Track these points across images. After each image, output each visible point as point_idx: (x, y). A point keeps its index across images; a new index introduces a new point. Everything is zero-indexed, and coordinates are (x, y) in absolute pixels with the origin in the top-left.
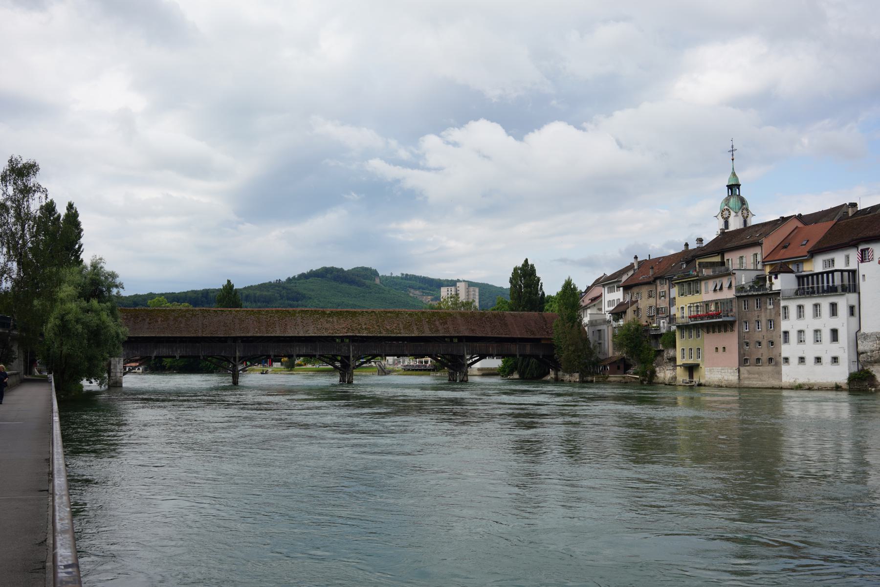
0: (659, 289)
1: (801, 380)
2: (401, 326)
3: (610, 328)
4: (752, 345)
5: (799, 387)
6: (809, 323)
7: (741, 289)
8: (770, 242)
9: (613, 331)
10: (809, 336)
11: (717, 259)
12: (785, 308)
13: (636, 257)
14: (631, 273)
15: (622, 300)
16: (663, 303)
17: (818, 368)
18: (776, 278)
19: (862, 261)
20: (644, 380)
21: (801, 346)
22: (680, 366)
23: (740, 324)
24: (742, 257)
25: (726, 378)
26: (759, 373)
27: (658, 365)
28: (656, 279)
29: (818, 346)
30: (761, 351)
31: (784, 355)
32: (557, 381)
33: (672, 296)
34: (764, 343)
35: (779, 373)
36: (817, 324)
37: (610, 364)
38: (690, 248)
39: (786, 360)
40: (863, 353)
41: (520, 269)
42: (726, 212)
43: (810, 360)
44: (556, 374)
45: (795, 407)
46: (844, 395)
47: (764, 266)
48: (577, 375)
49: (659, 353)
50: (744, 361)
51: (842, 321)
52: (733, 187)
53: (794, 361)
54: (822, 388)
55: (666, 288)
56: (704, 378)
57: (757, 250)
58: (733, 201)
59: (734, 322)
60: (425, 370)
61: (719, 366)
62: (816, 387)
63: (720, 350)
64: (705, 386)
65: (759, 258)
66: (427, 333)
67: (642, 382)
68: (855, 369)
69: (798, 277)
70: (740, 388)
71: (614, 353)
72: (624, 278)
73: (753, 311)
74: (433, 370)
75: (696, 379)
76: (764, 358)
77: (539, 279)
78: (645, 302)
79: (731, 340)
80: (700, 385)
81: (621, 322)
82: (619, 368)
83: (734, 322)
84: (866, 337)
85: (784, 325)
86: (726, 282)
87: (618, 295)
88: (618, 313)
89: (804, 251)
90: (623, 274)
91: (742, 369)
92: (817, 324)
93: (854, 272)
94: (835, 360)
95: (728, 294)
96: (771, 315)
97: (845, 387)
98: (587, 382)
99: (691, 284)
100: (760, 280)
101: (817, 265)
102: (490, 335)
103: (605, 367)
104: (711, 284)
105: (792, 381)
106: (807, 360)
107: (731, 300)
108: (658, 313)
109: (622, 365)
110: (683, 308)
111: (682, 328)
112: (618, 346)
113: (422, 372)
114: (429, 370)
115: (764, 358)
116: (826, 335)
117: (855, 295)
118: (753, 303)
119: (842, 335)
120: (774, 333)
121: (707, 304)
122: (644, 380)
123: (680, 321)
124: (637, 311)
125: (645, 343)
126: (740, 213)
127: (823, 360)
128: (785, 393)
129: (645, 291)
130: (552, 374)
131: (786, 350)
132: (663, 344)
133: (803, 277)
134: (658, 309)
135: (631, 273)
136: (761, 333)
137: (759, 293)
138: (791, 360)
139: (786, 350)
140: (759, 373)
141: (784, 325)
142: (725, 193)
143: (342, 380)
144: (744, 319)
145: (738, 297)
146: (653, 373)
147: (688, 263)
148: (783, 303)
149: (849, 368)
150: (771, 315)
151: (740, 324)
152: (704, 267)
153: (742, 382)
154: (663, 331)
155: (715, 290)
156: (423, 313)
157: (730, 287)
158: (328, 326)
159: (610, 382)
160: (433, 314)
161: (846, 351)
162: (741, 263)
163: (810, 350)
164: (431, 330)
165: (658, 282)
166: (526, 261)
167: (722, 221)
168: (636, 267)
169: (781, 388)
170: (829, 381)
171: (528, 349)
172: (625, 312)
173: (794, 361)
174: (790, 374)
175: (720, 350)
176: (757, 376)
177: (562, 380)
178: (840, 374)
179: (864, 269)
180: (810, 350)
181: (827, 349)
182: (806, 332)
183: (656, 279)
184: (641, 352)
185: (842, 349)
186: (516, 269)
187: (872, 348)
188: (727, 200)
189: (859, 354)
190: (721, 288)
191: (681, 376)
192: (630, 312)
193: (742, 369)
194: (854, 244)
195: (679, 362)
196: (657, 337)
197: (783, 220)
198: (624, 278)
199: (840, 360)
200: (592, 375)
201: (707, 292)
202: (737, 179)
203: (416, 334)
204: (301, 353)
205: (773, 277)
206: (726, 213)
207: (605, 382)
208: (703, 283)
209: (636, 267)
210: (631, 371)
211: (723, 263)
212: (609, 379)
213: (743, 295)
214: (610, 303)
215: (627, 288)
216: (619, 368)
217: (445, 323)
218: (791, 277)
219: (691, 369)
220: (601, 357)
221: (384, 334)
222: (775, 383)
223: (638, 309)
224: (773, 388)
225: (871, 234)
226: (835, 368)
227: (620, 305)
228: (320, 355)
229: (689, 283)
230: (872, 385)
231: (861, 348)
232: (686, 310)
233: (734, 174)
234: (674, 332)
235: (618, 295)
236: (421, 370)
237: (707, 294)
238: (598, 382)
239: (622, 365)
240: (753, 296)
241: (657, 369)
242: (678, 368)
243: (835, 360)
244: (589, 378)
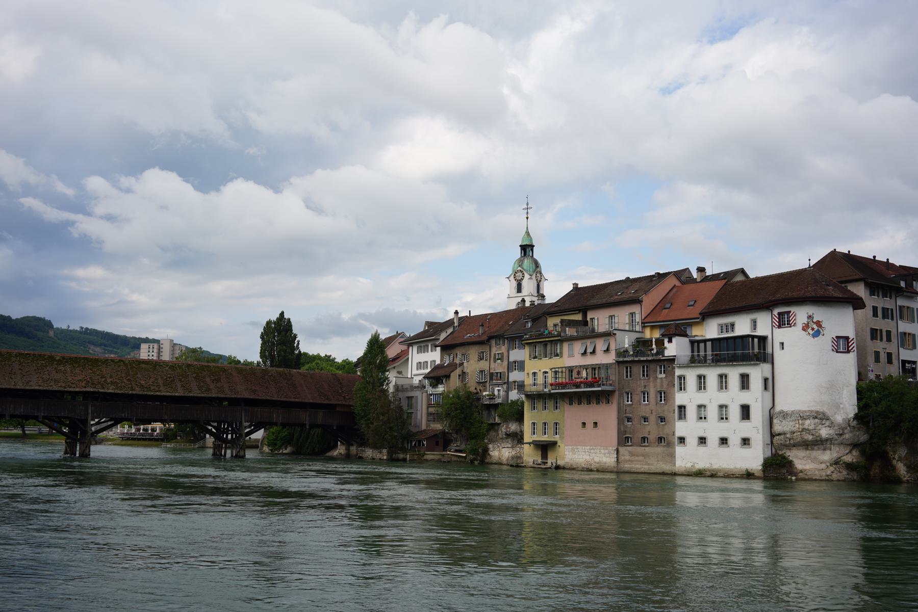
0: (494, 350)
1: (701, 465)
2: (160, 382)
3: (425, 394)
4: (636, 421)
5: (700, 474)
6: (712, 396)
7: (622, 353)
8: (651, 300)
9: (429, 399)
10: (712, 412)
11: (578, 317)
12: (680, 377)
13: (456, 313)
14: (450, 330)
15: (438, 362)
16: (499, 367)
17: (724, 450)
18: (670, 341)
19: (779, 327)
20: (475, 459)
21: (702, 424)
22: (529, 443)
23: (621, 395)
24: (611, 317)
25: (597, 459)
26: (645, 455)
27: (491, 441)
28: (490, 338)
29: (724, 424)
30: (648, 428)
31: (679, 433)
32: (348, 458)
33: (511, 359)
34: (653, 419)
35: (672, 456)
36: (723, 398)
37: (427, 439)
38: (528, 304)
39: (682, 440)
40: (779, 434)
41: (275, 323)
42: (520, 274)
43: (713, 441)
44: (348, 449)
45: (689, 498)
46: (758, 485)
47: (644, 327)
48: (385, 451)
49: (494, 426)
50: (624, 440)
51: (755, 397)
52: (527, 249)
53: (692, 441)
54: (729, 476)
55: (504, 349)
56: (563, 458)
57: (636, 309)
58: (527, 262)
59: (613, 392)
60: (150, 440)
61: (587, 445)
62: (721, 474)
63: (590, 425)
64: (564, 468)
65: (638, 318)
66: (196, 393)
67: (472, 462)
68: (769, 454)
69: (692, 343)
70: (619, 472)
71: (427, 425)
72: (443, 336)
73: (639, 382)
74: (162, 440)
75: (550, 461)
76: (652, 437)
77: (295, 336)
78: (473, 365)
79: (608, 415)
80: (558, 468)
81: (441, 389)
82: (437, 444)
83: (613, 392)
84: (784, 415)
85: (680, 398)
86: (601, 345)
87: (434, 356)
88: (437, 376)
89: (695, 312)
90: (441, 331)
91: (621, 449)
92: (723, 398)
93: (763, 339)
94: (746, 442)
95: (602, 358)
96: (662, 385)
97: (760, 474)
98: (398, 460)
99: (547, 344)
100: (642, 344)
101: (711, 330)
102: (275, 398)
103: (419, 442)
104: (578, 347)
105: (689, 465)
106: (709, 441)
107: (607, 366)
108: (491, 379)
109: (441, 441)
110: (534, 374)
111: (531, 397)
112: (433, 417)
113: (146, 443)
114: (157, 440)
115: (652, 437)
116: (735, 412)
117: (766, 367)
118: (637, 370)
119: (757, 413)
120: (666, 407)
121: (571, 370)
122: (475, 459)
123: (530, 389)
124: (463, 375)
125: (476, 414)
126: (534, 276)
127: (730, 442)
128: (680, 480)
129: (473, 352)
130: (341, 450)
131: (680, 428)
132: (499, 416)
133: (699, 342)
134: (491, 375)
135: (450, 330)
136: (648, 407)
137: (645, 359)
138: (687, 441)
139: (680, 428)
140: (645, 455)
141: (680, 398)
142: (518, 253)
143: (70, 449)
144: (630, 387)
145: (618, 362)
146: (486, 450)
147: (534, 320)
148: (678, 372)
149: (764, 453)
150: (662, 385)
151: (621, 395)
152: (567, 326)
153: (621, 465)
154: (499, 401)
155: (585, 353)
156: (189, 366)
157: (607, 350)
158: (58, 376)
159: (427, 460)
160: (203, 368)
161: (761, 431)
162: (611, 323)
163: (713, 429)
164: (200, 388)
165: (493, 342)
166: (282, 314)
167: (515, 284)
168: (456, 324)
169: (675, 474)
170: (738, 466)
171: (320, 418)
172: (448, 377)
173: (692, 441)
174: (686, 457)
175: (590, 425)
176: (641, 458)
177: (361, 458)
178: (753, 459)
179: (780, 335)
180: (713, 429)
181: (735, 428)
182: (709, 408)
183: (490, 338)
184: (471, 424)
185: (755, 428)
186: (269, 323)
187: (793, 429)
188: (520, 262)
189: (772, 436)
190: (594, 352)
191: (530, 455)
192: (455, 376)
193: (621, 449)
194: (766, 306)
195: (528, 437)
196: (489, 407)
197: (660, 277)
198: (443, 336)
199: (752, 442)
200: (405, 451)
201: (571, 355)
202: (531, 240)
203: (180, 393)
204: (17, 413)
205: (666, 341)
206: (519, 275)
207: (419, 462)
208: (566, 346)
209: (456, 324)
210: (453, 446)
211: (585, 323)
212: (426, 457)
213: (624, 362)
214: (420, 365)
215: (446, 348)
216: (437, 444)
217: (218, 380)
218: (685, 341)
219: (545, 448)
220: (414, 430)
221: (137, 391)
222: (667, 468)
223: (464, 373)
224: (663, 474)
225: (795, 294)
226: (746, 451)
227: (436, 368)
228: (44, 417)
229: (545, 344)
230: (792, 474)
231: (778, 428)
232: (550, 375)
233: (528, 233)
234: (523, 403)
235: (434, 356)
236: (139, 439)
237: (572, 357)
238: (412, 461)
239: (441, 441)
240: (640, 361)
241: (490, 446)
242: (526, 446)
243: (746, 442)
244: (401, 456)
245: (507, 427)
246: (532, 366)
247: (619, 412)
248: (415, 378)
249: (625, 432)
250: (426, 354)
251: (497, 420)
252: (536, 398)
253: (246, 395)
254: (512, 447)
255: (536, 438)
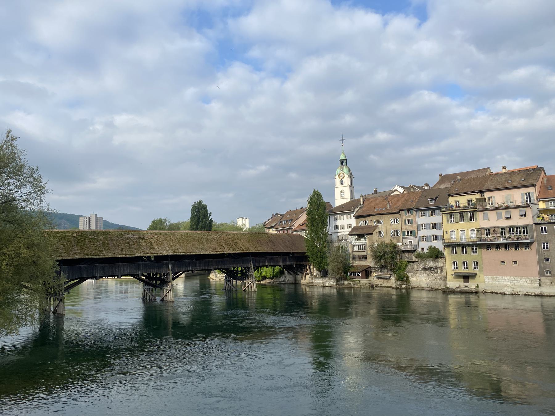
23: (539, 244)
50: (543, 272)
55: (411, 217)
79: (530, 257)
83: (531, 243)
132: (416, 257)
172: (371, 234)
192: (375, 233)
227: (354, 229)
241: (410, 275)
245: (425, 264)
246: (448, 227)
247: (539, 254)
248: (333, 235)
249: (545, 268)
250: (342, 220)
251: (414, 259)
252: (453, 246)
253: (253, 250)
254: (428, 275)
255: (457, 271)
